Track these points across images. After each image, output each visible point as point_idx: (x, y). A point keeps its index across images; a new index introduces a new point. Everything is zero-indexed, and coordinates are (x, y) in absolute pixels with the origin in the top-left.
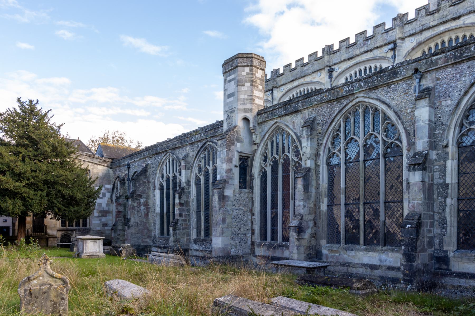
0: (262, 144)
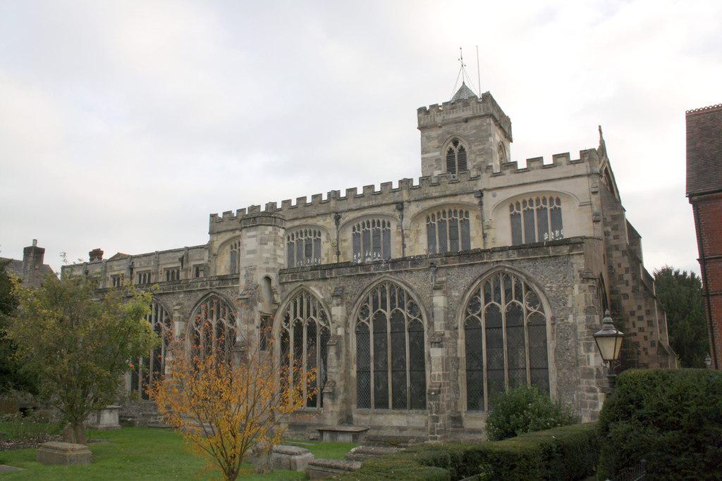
0: (284, 305)
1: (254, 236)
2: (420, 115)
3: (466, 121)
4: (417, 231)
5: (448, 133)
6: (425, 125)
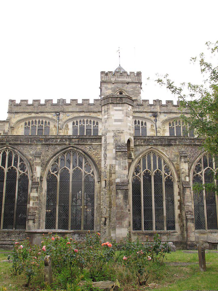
1: (120, 110)
2: (102, 75)
3: (128, 83)
4: (164, 130)
5: (118, 88)
6: (105, 81)
